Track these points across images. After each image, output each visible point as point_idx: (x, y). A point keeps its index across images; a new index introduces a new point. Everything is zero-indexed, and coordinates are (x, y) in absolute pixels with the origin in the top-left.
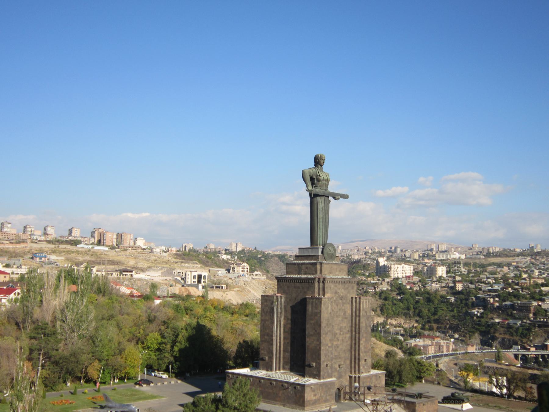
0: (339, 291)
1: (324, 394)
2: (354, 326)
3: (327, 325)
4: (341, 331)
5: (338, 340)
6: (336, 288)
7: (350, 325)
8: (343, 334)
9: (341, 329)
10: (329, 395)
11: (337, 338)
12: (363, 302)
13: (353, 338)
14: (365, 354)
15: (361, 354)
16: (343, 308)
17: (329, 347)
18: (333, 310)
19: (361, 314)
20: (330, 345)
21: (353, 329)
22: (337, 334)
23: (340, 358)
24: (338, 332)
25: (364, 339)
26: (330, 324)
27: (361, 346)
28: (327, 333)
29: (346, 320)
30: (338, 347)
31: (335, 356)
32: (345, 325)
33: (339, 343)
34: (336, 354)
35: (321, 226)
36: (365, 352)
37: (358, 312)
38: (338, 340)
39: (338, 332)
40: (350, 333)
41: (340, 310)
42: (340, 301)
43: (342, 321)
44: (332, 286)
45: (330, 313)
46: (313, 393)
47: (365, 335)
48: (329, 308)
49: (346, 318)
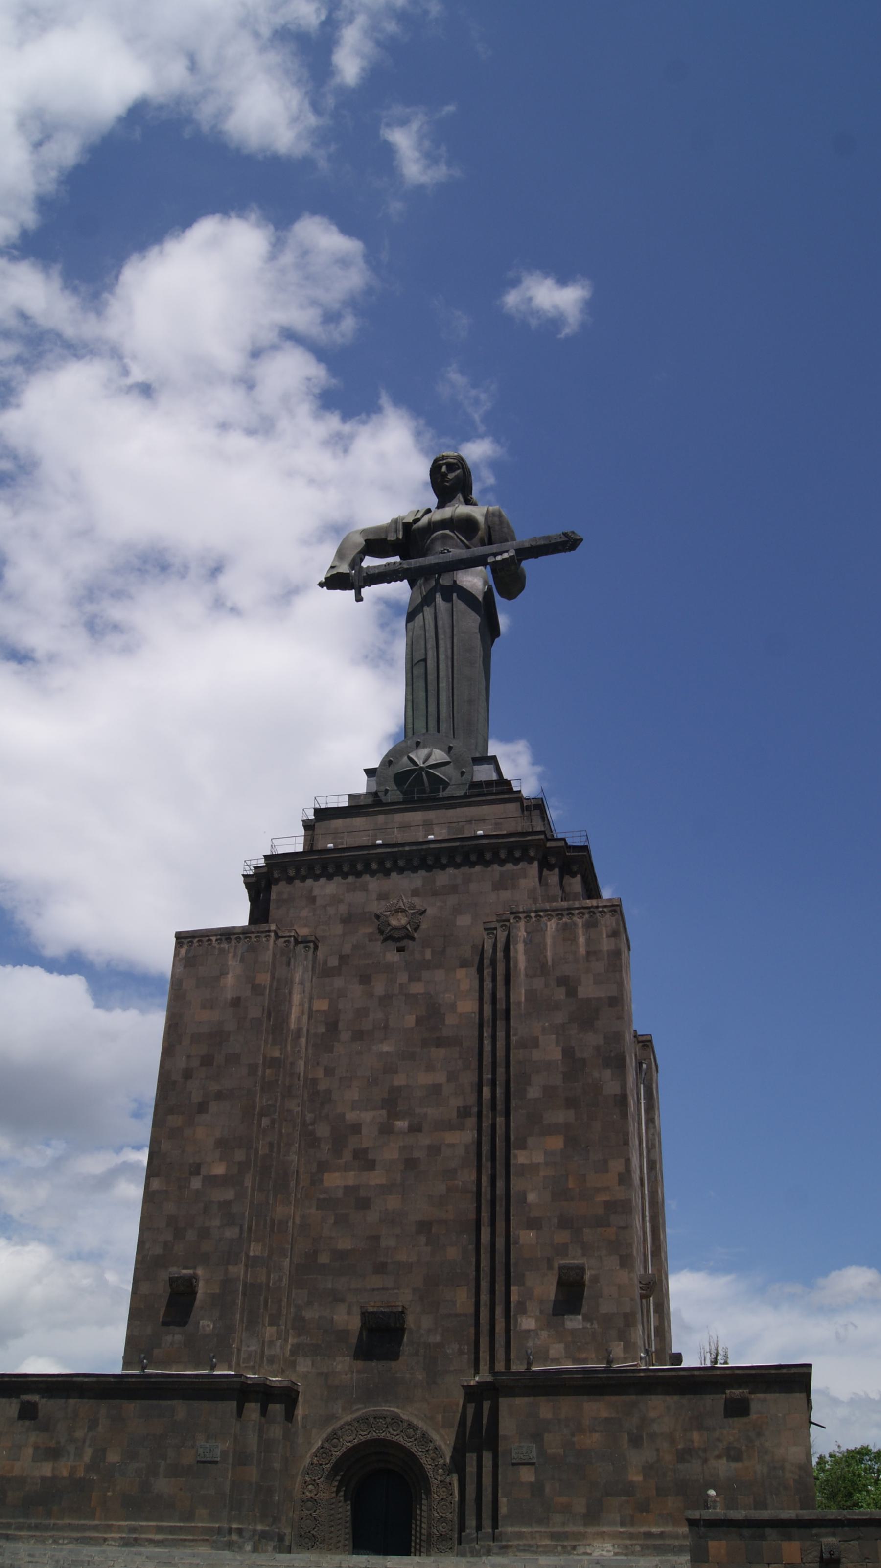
0: (376, 907)
2: (487, 1076)
3: (207, 1061)
4: (394, 1115)
5: (364, 1161)
8: (415, 1129)
9: (392, 1103)
12: (535, 932)
13: (486, 1148)
14: (562, 1237)
15: (526, 1237)
16: (417, 988)
17: (211, 1181)
18: (257, 989)
19: (519, 994)
20: (219, 1170)
21: (486, 1091)
22: (356, 1128)
23: (380, 1269)
25: (556, 1143)
27: (516, 1184)
28: (202, 1108)
30: (364, 1204)
31: (340, 1255)
32: (440, 1077)
33: (376, 1178)
34: (345, 1244)
35: (422, 694)
36: (565, 1223)
37: (501, 994)
38: (364, 1161)
40: (472, 1121)
41: (386, 1000)
42: (393, 957)
44: (326, 889)
45: (236, 1002)
46: (33, 1438)
47: (560, 1116)
48: (230, 980)
49: (440, 1043)
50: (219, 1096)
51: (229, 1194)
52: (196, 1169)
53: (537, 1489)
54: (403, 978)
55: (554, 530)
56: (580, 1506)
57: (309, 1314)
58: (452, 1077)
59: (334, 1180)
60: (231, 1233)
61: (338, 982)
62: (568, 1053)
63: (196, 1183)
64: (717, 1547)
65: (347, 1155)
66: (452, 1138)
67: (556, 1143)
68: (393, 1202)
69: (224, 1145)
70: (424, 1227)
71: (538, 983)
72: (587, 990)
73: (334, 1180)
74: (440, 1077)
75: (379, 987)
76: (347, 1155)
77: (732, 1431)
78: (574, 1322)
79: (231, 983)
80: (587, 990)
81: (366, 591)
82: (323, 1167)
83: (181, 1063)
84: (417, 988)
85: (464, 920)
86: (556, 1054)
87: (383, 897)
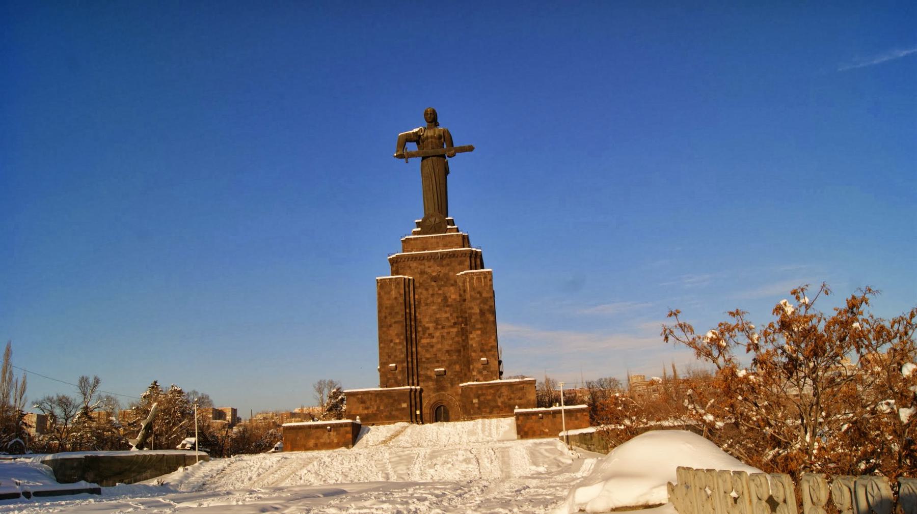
0: (429, 271)
1: (386, 406)
3: (390, 314)
5: (431, 336)
6: (423, 267)
7: (455, 315)
9: (437, 322)
10: (397, 410)
11: (429, 334)
15: (473, 354)
16: (440, 292)
17: (395, 344)
19: (468, 296)
20: (397, 341)
22: (428, 328)
23: (438, 362)
24: (431, 325)
25: (479, 332)
26: (397, 313)
27: (470, 342)
28: (390, 326)
29: (448, 309)
30: (432, 347)
31: (428, 359)
32: (448, 315)
33: (434, 340)
34: (428, 356)
38: (431, 336)
39: (431, 325)
41: (433, 295)
42: (433, 283)
43: (439, 309)
44: (414, 264)
45: (396, 298)
47: (479, 326)
48: (393, 292)
49: (448, 306)
50: (395, 322)
51: (401, 347)
52: (391, 341)
53: (479, 408)
54: (436, 289)
55: (466, 144)
56: (488, 410)
57: (421, 373)
58: (451, 315)
59: (424, 341)
60: (403, 356)
61: (420, 290)
62: (481, 310)
63: (392, 345)
64: (521, 418)
65: (427, 335)
66: (452, 330)
67: (479, 332)
68: (439, 346)
69: (398, 335)
70: (447, 351)
71: (473, 293)
72: (485, 295)
73: (424, 341)
74: (448, 315)
75: (431, 292)
76: (427, 335)
77: (519, 395)
78: (485, 373)
79: (394, 293)
80: (485, 295)
81: (409, 160)
82: (421, 338)
83: (384, 315)
84: (440, 292)
85: (451, 274)
86: (478, 311)
87: (430, 267)
